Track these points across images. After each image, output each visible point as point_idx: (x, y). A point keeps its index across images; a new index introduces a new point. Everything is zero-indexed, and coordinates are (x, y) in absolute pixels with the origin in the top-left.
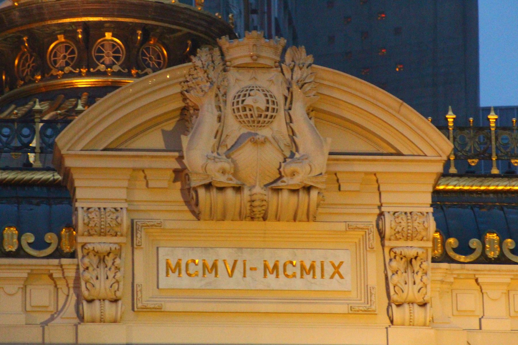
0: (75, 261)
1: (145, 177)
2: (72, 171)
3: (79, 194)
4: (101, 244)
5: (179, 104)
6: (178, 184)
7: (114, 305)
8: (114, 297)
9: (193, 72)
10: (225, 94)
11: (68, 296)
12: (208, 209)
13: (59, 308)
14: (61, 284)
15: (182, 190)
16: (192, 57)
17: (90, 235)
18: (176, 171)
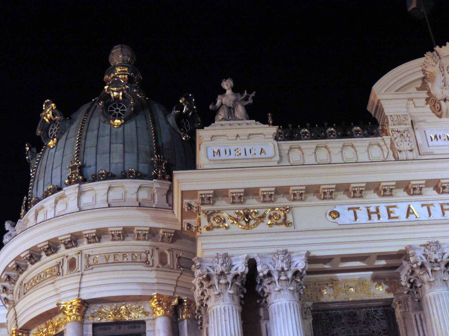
0: (389, 137)
1: (413, 103)
2: (381, 101)
3: (386, 111)
4: (401, 128)
5: (422, 75)
6: (428, 106)
7: (411, 152)
8: (410, 149)
9: (426, 60)
10: (443, 67)
11: (388, 152)
12: (446, 111)
13: (385, 157)
14: (384, 147)
15: (431, 108)
16: (425, 55)
17: (394, 125)
18: (427, 100)
